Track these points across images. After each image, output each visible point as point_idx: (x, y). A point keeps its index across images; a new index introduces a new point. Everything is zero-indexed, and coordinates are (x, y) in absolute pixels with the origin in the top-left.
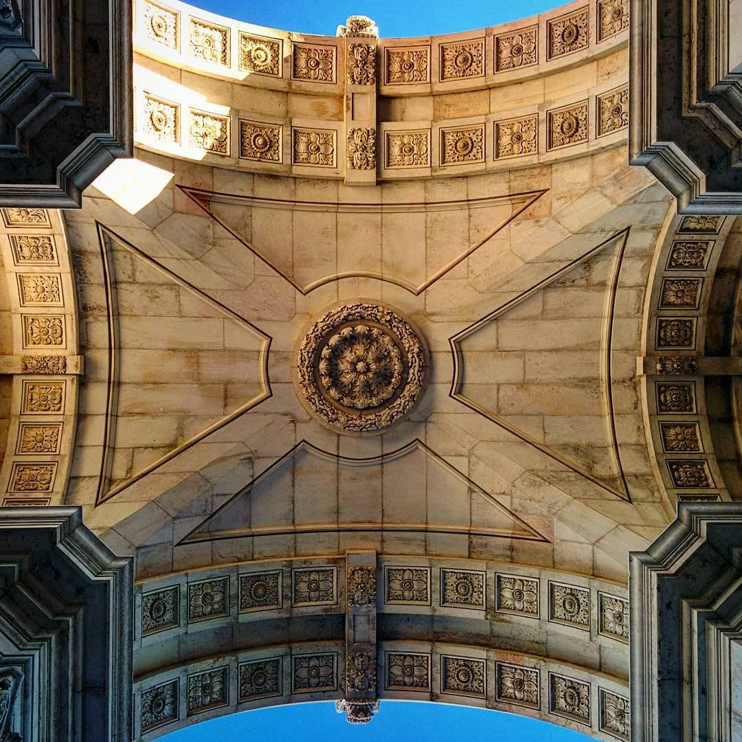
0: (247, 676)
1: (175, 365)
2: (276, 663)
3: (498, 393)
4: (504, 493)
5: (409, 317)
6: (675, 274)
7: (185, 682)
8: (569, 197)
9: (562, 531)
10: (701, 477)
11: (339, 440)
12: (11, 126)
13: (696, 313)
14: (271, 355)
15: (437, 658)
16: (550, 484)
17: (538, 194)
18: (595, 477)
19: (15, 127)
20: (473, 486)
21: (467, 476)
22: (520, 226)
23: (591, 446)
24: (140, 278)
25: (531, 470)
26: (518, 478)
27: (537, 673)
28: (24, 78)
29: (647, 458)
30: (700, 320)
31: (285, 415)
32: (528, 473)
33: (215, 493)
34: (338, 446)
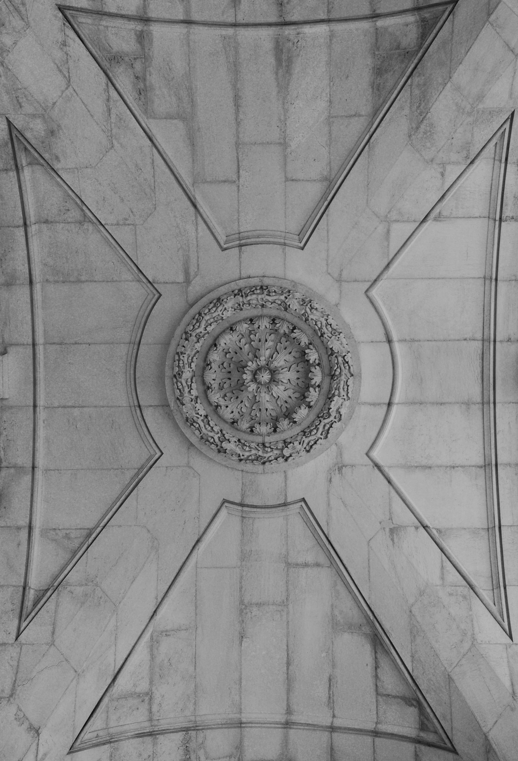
4: (442, 175)
14: (247, 501)
17: (15, 132)
18: (420, 48)
20: (432, 215)
21: (418, 224)
22: (60, 155)
24: (143, 686)
31: (330, 481)
33: (439, 582)
34: (374, 404)
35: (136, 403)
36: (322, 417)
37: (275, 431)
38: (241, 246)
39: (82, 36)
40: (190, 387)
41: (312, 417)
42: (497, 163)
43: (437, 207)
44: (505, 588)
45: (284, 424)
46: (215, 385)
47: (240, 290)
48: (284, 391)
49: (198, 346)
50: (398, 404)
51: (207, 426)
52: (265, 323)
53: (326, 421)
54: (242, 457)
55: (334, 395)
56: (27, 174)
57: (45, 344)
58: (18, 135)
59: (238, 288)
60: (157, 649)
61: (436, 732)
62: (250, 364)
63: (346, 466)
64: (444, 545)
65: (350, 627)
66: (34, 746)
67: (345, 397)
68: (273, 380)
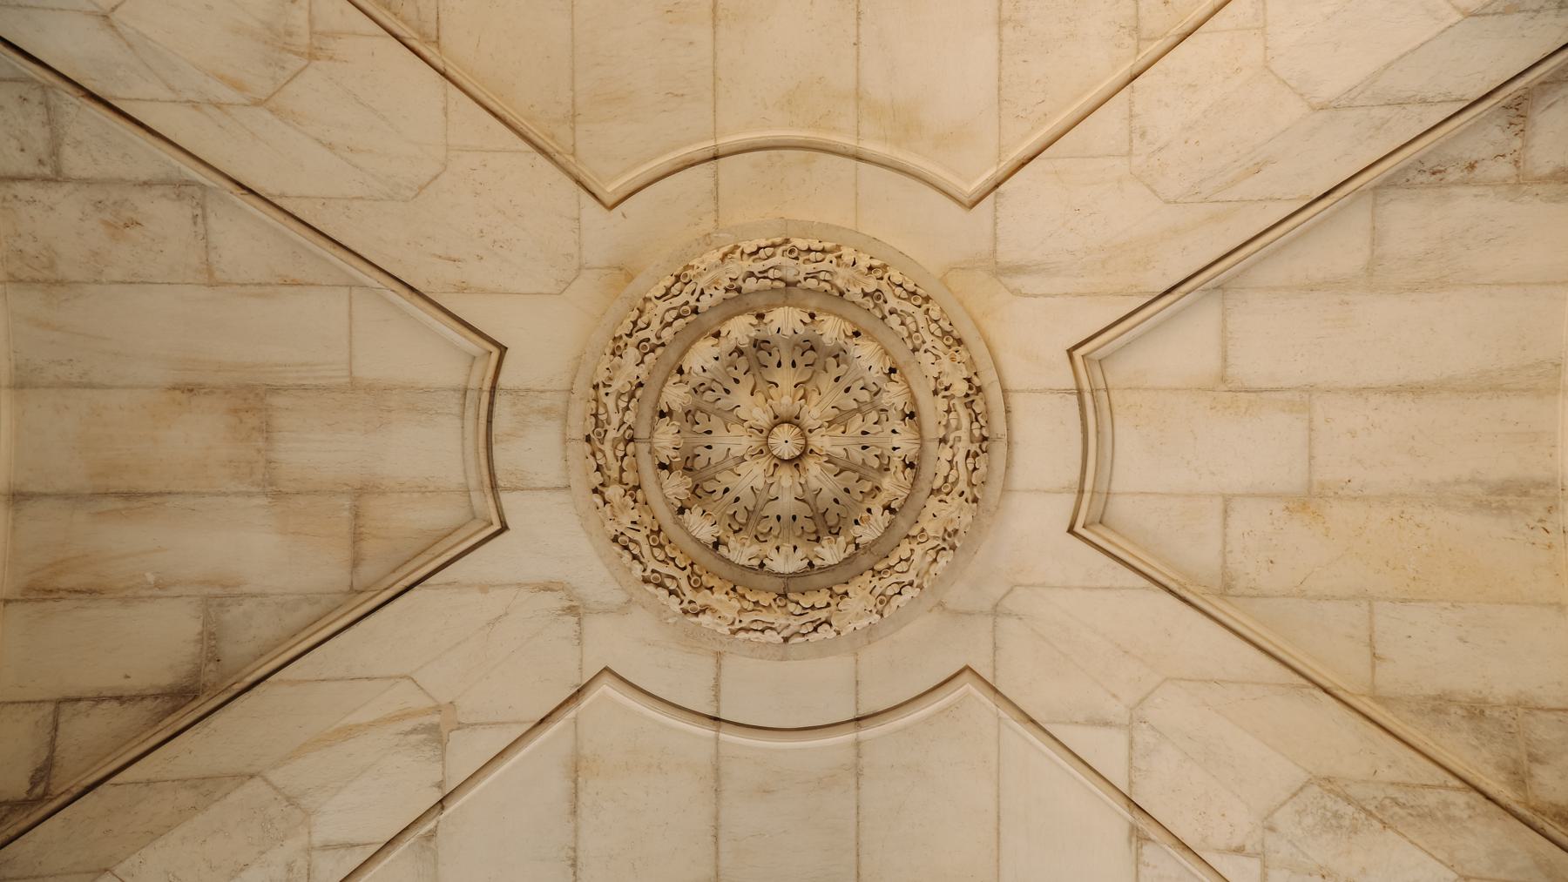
3: (1225, 525)
4: (1240, 850)
5: (943, 281)
11: (719, 666)
14: (501, 402)
16: (1385, 825)
20: (1142, 823)
24: (74, 161)
25: (1329, 780)
26: (1283, 804)
32: (1317, 789)
33: (317, 839)
34: (717, 687)
36: (693, 572)
37: (662, 466)
38: (1080, 392)
41: (693, 549)
43: (1160, 831)
45: (677, 486)
48: (752, 487)
50: (717, 739)
51: (674, 314)
52: (904, 442)
53: (684, 583)
54: (602, 391)
59: (985, 386)
60: (164, 196)
63: (579, 623)
65: (211, 639)
67: (737, 626)
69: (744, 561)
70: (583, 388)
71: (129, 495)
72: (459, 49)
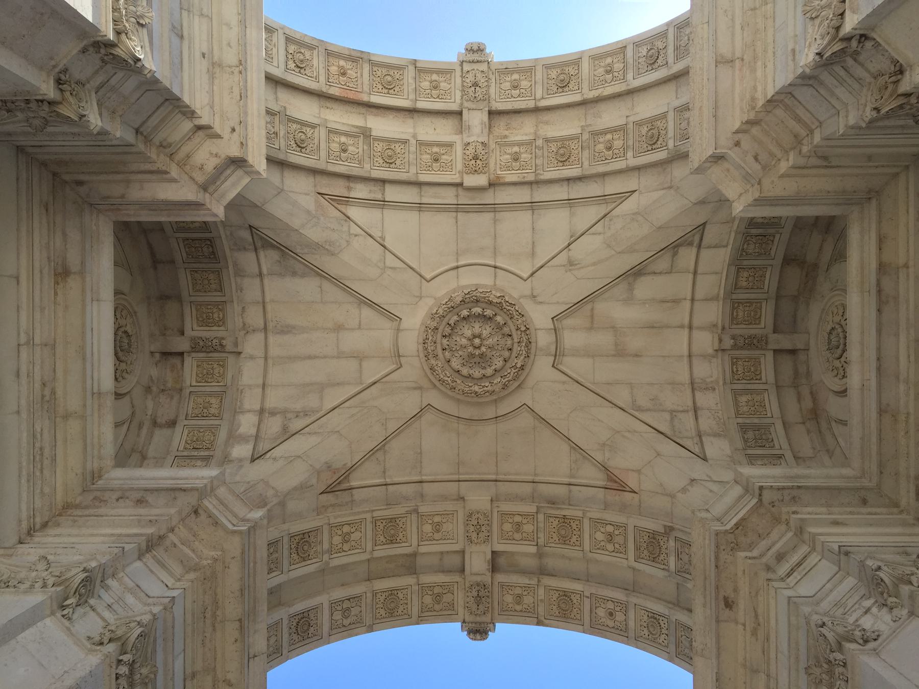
0: (573, 82)
1: (635, 343)
2: (548, 92)
3: (360, 321)
4: (356, 236)
6: (211, 422)
7: (628, 76)
8: (302, 488)
9: (308, 202)
10: (189, 248)
12: (799, 534)
13: (192, 389)
14: (554, 353)
15: (412, 96)
17: (328, 490)
19: (795, 534)
20: (382, 242)
23: (281, 275)
24: (667, 416)
25: (332, 255)
27: (328, 82)
28: (789, 575)
29: (235, 264)
30: (188, 383)
32: (336, 252)
34: (495, 276)
35: (495, 419)
37: (510, 336)
38: (399, 356)
39: (271, 448)
40: (484, 387)
41: (501, 313)
42: (349, 203)
44: (606, 196)
45: (506, 330)
46: (483, 372)
47: (426, 356)
49: (459, 382)
52: (445, 341)
53: (504, 305)
55: (488, 300)
56: (354, 484)
57: (459, 473)
58: (331, 487)
61: (694, 236)
62: (469, 350)
63: (532, 294)
64: (579, 233)
65: (631, 289)
66: (703, 482)
68: (479, 336)
69: (488, 311)
70: (532, 356)
71: (653, 327)
72: (565, 447)
